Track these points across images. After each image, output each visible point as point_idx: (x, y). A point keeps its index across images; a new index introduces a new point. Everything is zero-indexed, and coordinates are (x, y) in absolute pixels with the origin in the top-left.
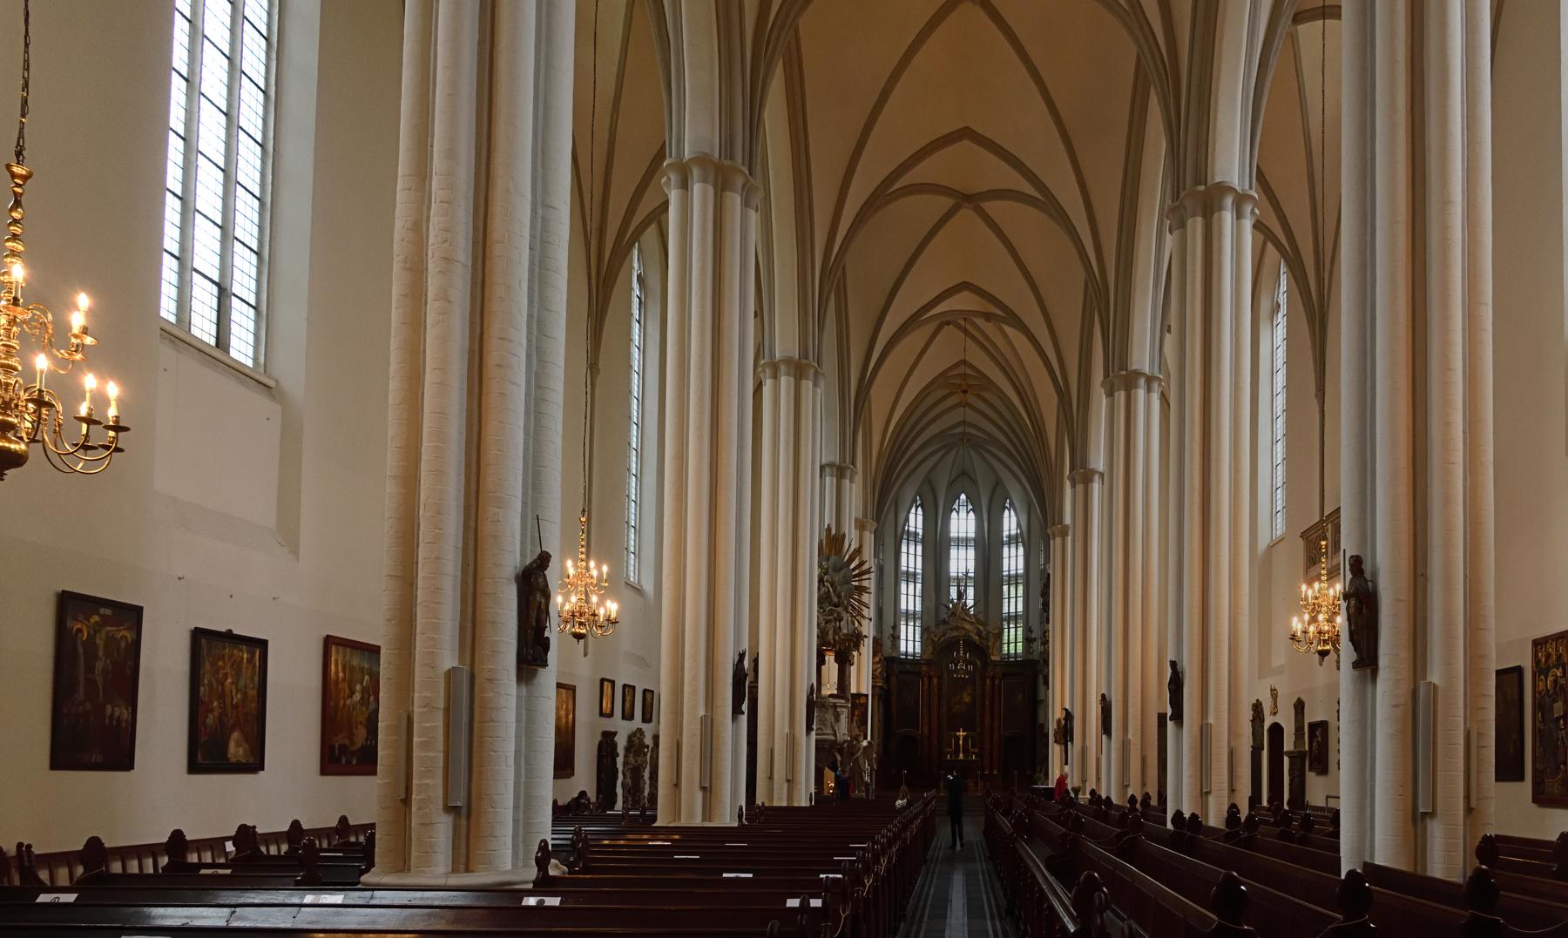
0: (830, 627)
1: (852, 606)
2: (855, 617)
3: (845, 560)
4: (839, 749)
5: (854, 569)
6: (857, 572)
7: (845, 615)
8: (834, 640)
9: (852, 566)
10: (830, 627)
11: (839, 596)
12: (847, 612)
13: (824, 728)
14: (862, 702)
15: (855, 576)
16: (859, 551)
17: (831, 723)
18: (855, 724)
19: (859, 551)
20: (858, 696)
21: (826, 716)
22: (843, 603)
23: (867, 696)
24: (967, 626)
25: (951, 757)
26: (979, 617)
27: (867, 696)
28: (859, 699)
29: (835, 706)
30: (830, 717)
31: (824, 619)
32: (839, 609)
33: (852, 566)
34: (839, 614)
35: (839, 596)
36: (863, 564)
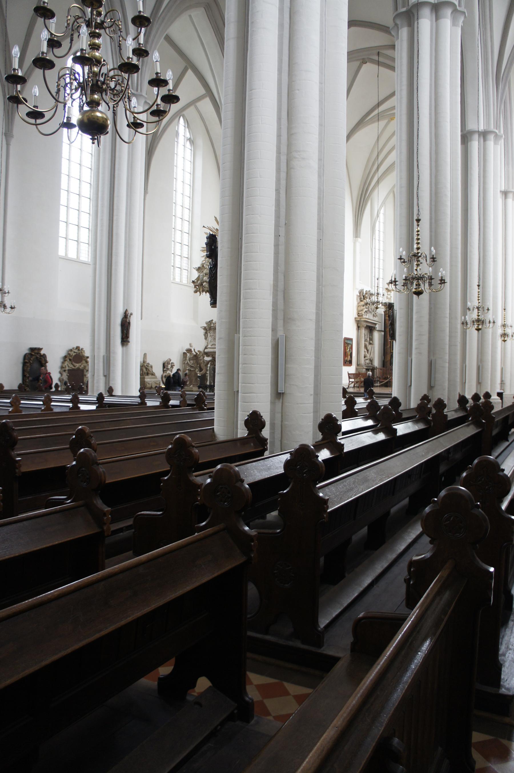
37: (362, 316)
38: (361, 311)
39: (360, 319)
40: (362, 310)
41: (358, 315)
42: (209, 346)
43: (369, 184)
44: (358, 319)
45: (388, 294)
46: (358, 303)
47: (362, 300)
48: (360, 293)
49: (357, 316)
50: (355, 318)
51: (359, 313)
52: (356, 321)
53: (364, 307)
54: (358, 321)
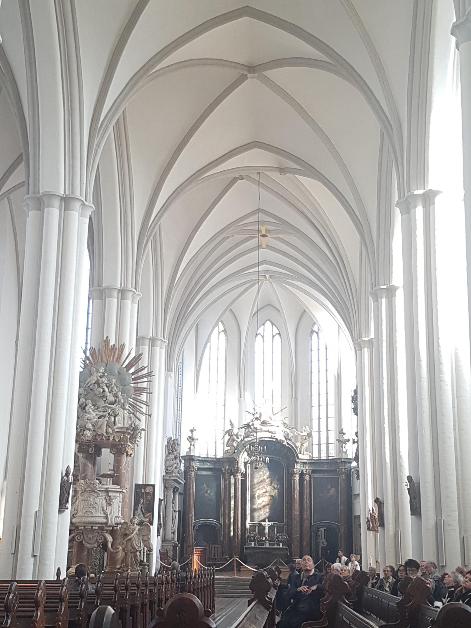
0: (104, 421)
1: (130, 404)
2: (133, 414)
3: (124, 366)
4: (111, 531)
5: (133, 374)
6: (136, 376)
7: (120, 412)
8: (106, 432)
9: (132, 370)
10: (104, 421)
11: (116, 396)
12: (124, 409)
13: (93, 511)
14: (147, 491)
15: (133, 379)
16: (138, 358)
17: (102, 507)
18: (139, 510)
19: (138, 358)
20: (145, 486)
21: (97, 500)
22: (119, 401)
23: (154, 486)
24: (271, 429)
25: (255, 544)
26: (285, 421)
27: (154, 486)
28: (145, 489)
29: (107, 491)
30: (101, 500)
31: (96, 415)
32: (113, 406)
33: (132, 370)
34: (113, 410)
35: (116, 396)
36: (144, 369)
37: (171, 473)
38: (170, 467)
39: (170, 477)
40: (172, 466)
41: (167, 471)
42: (80, 514)
43: (189, 307)
44: (168, 478)
45: (191, 445)
46: (167, 456)
47: (170, 451)
48: (168, 443)
49: (165, 474)
50: (164, 476)
51: (167, 470)
52: (163, 479)
53: (174, 461)
54: (166, 480)
